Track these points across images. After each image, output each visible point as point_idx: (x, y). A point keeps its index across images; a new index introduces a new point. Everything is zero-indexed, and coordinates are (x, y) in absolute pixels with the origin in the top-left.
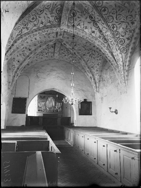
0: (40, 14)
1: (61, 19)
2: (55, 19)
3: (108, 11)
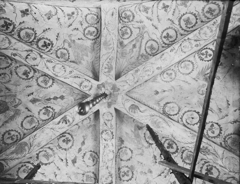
0: (169, 28)
1: (119, 16)
2: (134, 17)
3: (17, 74)
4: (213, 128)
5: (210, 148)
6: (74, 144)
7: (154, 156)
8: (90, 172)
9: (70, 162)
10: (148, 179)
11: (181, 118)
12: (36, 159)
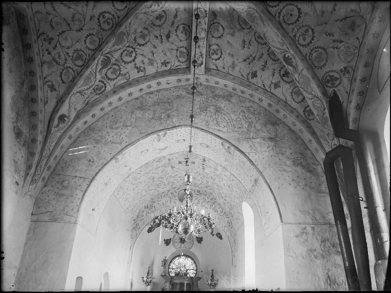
4: (307, 34)
5: (294, 60)
6: (167, 19)
7: (244, 40)
8: (183, 47)
9: (164, 38)
10: (234, 61)
11: (280, 13)
12: (134, 42)
